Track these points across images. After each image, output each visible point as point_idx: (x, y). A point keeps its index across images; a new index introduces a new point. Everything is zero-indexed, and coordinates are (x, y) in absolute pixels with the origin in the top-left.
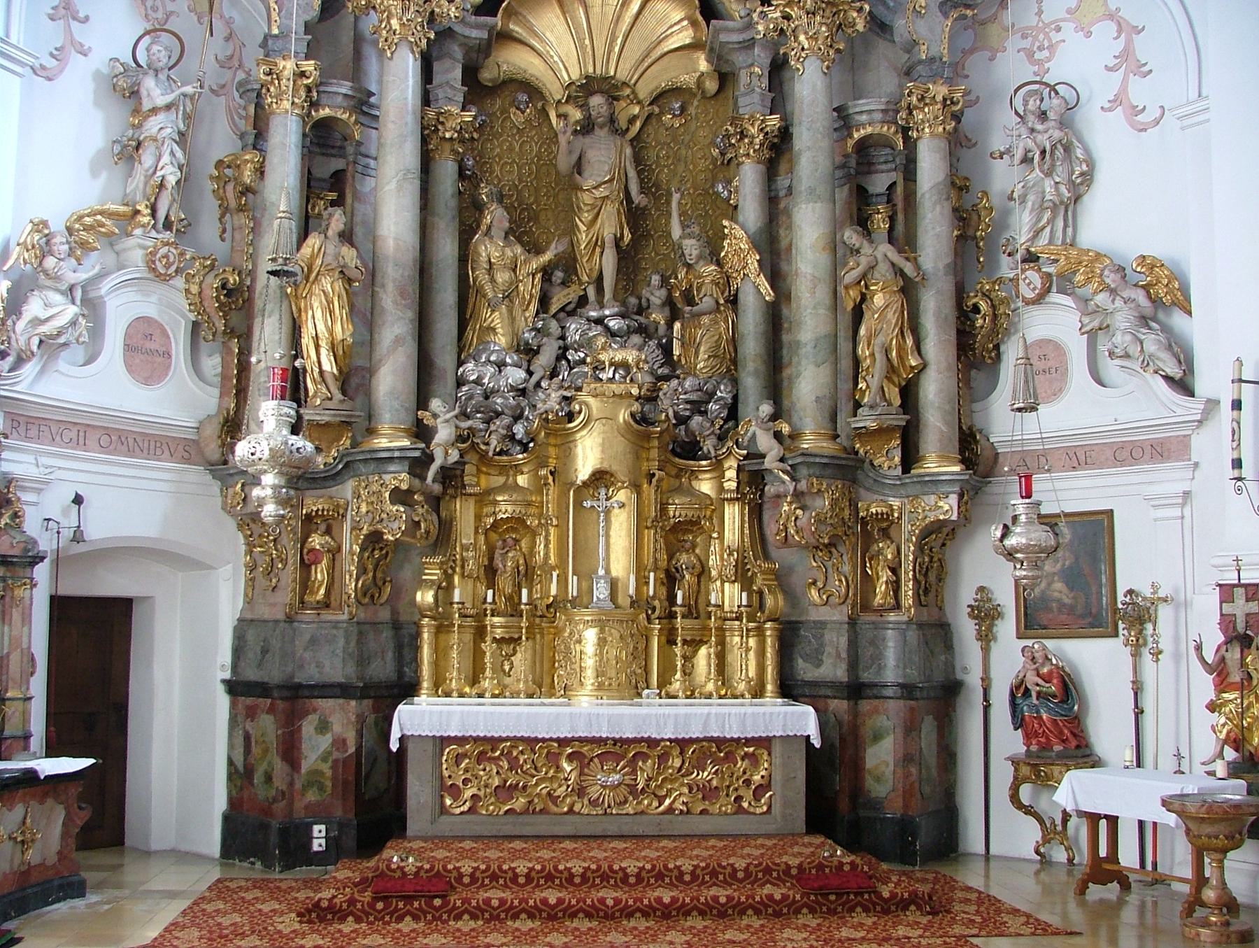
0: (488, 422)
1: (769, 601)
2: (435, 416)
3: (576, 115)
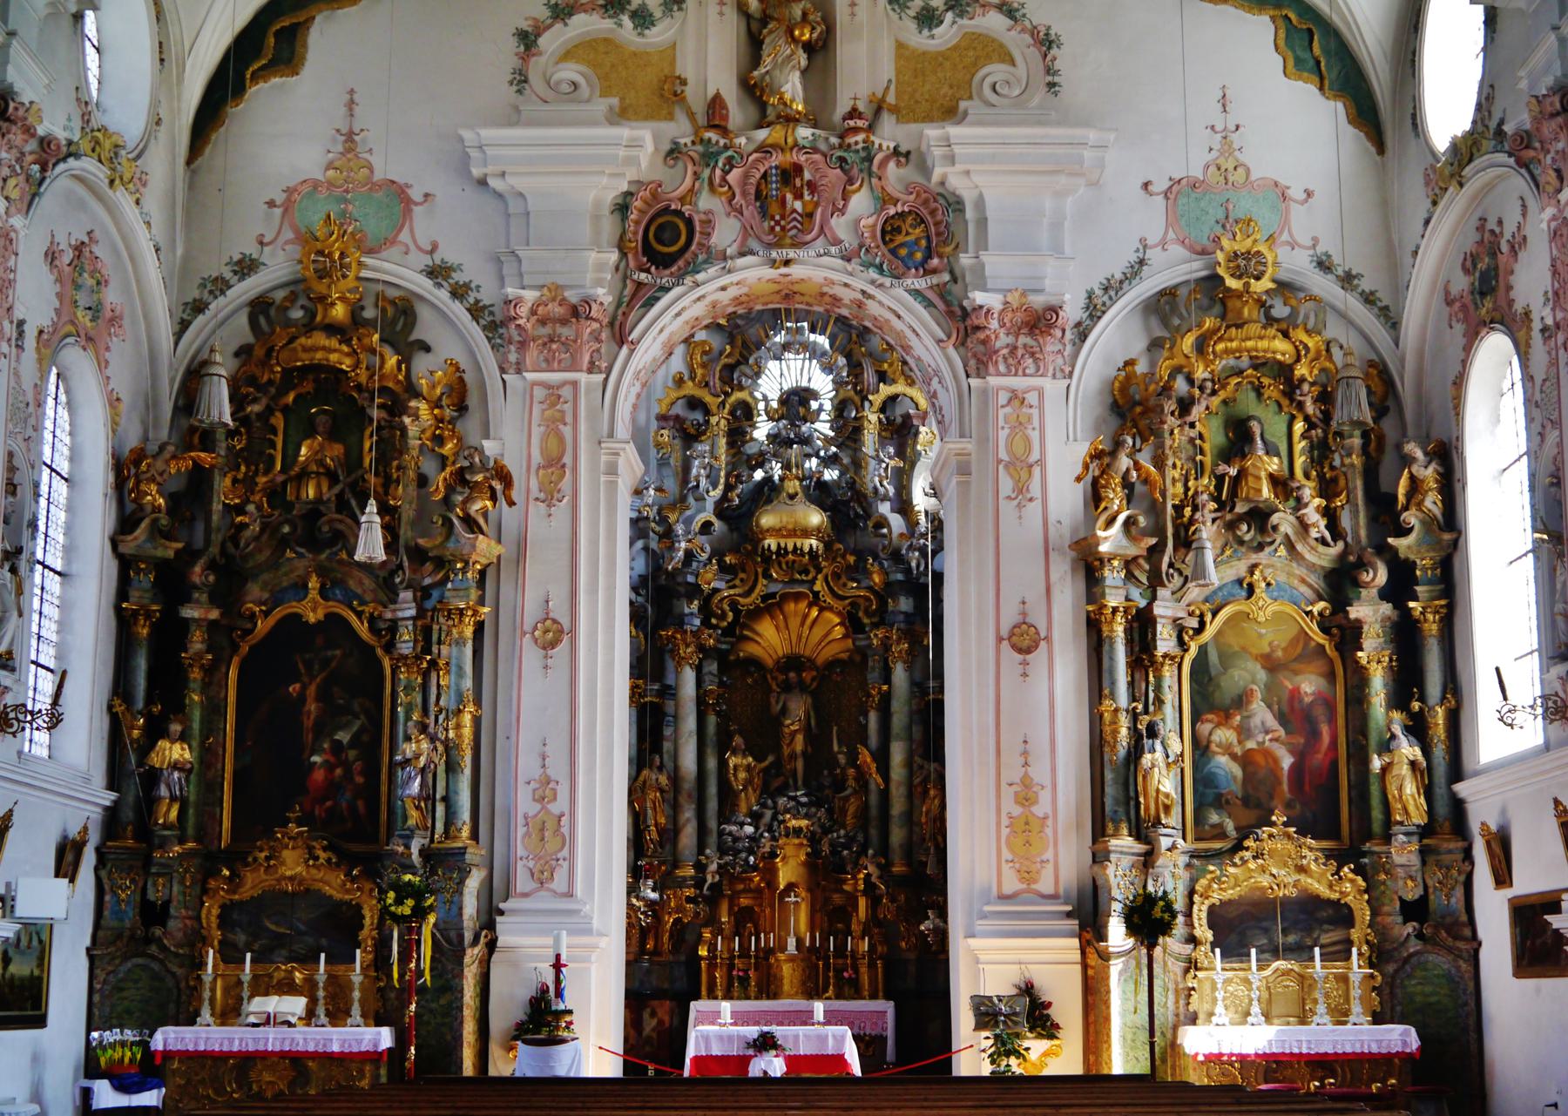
1: (879, 949)
2: (707, 858)
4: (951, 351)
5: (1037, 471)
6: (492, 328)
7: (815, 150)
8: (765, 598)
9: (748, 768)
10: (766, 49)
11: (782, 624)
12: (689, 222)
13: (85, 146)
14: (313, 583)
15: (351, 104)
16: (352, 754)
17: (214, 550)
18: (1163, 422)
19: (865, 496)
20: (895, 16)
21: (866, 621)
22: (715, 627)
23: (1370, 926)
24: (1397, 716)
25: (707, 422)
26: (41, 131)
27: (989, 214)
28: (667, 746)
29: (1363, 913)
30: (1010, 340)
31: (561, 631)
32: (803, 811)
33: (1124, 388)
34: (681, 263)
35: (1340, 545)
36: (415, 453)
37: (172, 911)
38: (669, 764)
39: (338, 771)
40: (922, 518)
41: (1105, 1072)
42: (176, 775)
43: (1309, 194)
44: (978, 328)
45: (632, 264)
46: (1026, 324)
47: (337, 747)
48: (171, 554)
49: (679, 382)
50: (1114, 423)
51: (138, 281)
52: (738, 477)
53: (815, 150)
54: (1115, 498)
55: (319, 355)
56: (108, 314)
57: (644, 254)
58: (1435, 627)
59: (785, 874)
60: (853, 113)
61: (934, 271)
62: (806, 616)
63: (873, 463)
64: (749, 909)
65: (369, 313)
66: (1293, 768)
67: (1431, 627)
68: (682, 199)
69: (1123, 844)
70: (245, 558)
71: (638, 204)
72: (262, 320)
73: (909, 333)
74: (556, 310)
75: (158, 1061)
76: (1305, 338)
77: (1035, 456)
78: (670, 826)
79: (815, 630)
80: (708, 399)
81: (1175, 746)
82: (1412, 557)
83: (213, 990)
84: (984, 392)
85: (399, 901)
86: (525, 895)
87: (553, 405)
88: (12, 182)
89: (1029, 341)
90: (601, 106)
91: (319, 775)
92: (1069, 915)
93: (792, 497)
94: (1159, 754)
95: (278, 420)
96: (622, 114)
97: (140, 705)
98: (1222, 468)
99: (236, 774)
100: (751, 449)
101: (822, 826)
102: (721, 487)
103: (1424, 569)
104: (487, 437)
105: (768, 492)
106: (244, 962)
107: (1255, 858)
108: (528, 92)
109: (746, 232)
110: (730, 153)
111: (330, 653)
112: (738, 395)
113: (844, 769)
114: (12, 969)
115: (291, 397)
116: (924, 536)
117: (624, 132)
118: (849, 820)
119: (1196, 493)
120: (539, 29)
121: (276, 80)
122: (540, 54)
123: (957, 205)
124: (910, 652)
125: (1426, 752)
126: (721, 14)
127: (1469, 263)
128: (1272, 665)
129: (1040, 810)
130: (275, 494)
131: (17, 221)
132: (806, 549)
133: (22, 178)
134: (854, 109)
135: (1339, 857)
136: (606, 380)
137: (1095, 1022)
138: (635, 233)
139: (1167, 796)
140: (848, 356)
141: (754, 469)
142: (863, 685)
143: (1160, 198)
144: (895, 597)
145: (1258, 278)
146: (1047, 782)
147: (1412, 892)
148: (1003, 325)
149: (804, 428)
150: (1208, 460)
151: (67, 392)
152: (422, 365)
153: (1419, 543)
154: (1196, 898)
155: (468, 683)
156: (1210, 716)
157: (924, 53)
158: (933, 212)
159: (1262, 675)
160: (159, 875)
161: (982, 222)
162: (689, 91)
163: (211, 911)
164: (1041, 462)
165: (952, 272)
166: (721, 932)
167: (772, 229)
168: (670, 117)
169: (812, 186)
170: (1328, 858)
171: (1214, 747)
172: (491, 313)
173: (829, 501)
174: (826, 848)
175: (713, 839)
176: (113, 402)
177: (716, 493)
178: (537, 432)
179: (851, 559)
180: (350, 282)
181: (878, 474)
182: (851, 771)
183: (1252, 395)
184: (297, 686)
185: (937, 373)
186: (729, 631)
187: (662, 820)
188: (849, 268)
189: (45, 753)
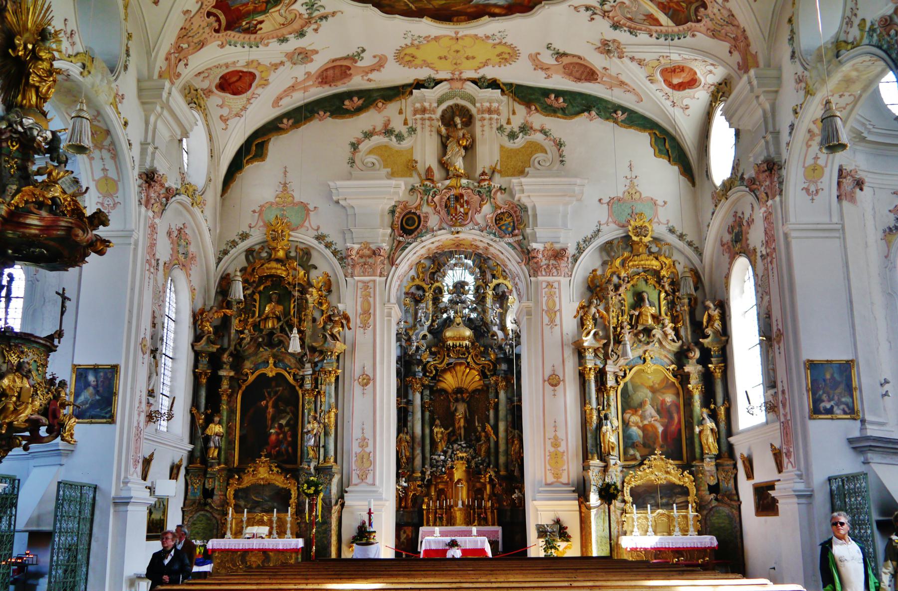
0: (437, 468)
3: (455, 396)
4: (523, 266)
5: (558, 314)
6: (341, 259)
7: (469, 188)
8: (448, 365)
9: (442, 433)
10: (449, 148)
11: (455, 375)
12: (419, 217)
13: (183, 190)
14: (271, 361)
15: (285, 172)
16: (286, 429)
17: (232, 348)
18: (608, 294)
19: (487, 324)
20: (499, 135)
21: (488, 373)
22: (428, 377)
23: (696, 495)
24: (705, 410)
25: (424, 295)
26: (166, 186)
27: (538, 212)
28: (409, 424)
29: (693, 490)
30: (547, 262)
31: (369, 379)
32: (464, 450)
33: (592, 280)
34: (416, 233)
35: (680, 342)
36: (311, 309)
37: (215, 493)
38: (410, 431)
39: (281, 436)
40: (510, 332)
41: (590, 555)
42: (217, 438)
43: (665, 203)
44: (534, 257)
45: (396, 234)
46: (553, 256)
47: (281, 426)
48: (215, 350)
49: (413, 279)
50: (588, 294)
51: (202, 243)
52: (437, 316)
53: (469, 188)
54: (590, 324)
55: (273, 271)
56: (191, 256)
57: (401, 229)
58: (719, 375)
59: (458, 474)
60: (483, 173)
61: (516, 235)
62: (464, 372)
63: (490, 311)
64: (442, 490)
65: (293, 254)
66: (663, 432)
67: (718, 374)
68: (416, 208)
69: (595, 462)
70: (244, 351)
71: (399, 210)
72: (250, 257)
73: (506, 260)
74: (367, 252)
75: (210, 553)
76: (665, 260)
77: (557, 308)
78: (411, 456)
79: (468, 377)
80: (425, 286)
81: (616, 423)
82: (710, 347)
83: (231, 524)
84: (537, 283)
85: (309, 488)
86: (356, 485)
87: (365, 290)
88: (155, 205)
89: (554, 262)
90: (384, 171)
91: (273, 437)
92: (574, 491)
93: (458, 324)
94: (609, 426)
95: (257, 297)
96: (392, 175)
97: (202, 410)
98: (632, 312)
99: (240, 437)
100: (442, 305)
101: (472, 456)
102: (430, 321)
103: (715, 351)
104: (340, 302)
105: (448, 322)
106: (244, 512)
107: (649, 468)
108: (355, 166)
109: (441, 220)
110: (435, 190)
111: (277, 389)
112: (436, 284)
113: (480, 433)
114: (153, 516)
115: (262, 288)
116: (510, 339)
117: (393, 182)
118: (483, 453)
119: (622, 322)
120: (359, 142)
121: (256, 163)
122: (360, 152)
123: (525, 209)
124: (506, 386)
125: (717, 424)
126: (431, 135)
127: (730, 230)
128: (653, 390)
129: (562, 448)
130: (256, 326)
131: (157, 221)
132: (464, 345)
133: (159, 204)
134: (484, 172)
135: (683, 467)
136: (387, 279)
137: (585, 535)
138: (398, 222)
139: (613, 443)
140: (480, 268)
141: (443, 313)
142: (488, 399)
143: (606, 206)
144: (500, 364)
145: (645, 236)
146: (564, 438)
147: (713, 482)
148: (544, 256)
149: (463, 297)
150: (626, 309)
151: (175, 287)
152: (314, 274)
153: (713, 341)
154: (625, 484)
155: (333, 400)
156: (629, 411)
157: (511, 150)
158: (515, 212)
159: (650, 394)
160: (210, 478)
161: (535, 216)
162: (419, 166)
163: (231, 492)
164: (560, 310)
165: (523, 235)
166: (431, 499)
167: (452, 219)
168: (411, 176)
169: (467, 202)
170: (678, 468)
171: (631, 423)
172: (341, 254)
173: (473, 326)
174: (473, 465)
175: (428, 461)
176: (193, 290)
177: (428, 323)
178: (359, 300)
179: (482, 349)
180: (285, 242)
181: (492, 315)
182: (483, 434)
183: (644, 283)
184: (265, 402)
185: (518, 275)
186: (434, 378)
187: (408, 454)
188: (482, 234)
189: (165, 430)
